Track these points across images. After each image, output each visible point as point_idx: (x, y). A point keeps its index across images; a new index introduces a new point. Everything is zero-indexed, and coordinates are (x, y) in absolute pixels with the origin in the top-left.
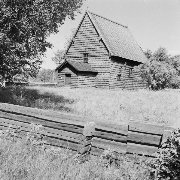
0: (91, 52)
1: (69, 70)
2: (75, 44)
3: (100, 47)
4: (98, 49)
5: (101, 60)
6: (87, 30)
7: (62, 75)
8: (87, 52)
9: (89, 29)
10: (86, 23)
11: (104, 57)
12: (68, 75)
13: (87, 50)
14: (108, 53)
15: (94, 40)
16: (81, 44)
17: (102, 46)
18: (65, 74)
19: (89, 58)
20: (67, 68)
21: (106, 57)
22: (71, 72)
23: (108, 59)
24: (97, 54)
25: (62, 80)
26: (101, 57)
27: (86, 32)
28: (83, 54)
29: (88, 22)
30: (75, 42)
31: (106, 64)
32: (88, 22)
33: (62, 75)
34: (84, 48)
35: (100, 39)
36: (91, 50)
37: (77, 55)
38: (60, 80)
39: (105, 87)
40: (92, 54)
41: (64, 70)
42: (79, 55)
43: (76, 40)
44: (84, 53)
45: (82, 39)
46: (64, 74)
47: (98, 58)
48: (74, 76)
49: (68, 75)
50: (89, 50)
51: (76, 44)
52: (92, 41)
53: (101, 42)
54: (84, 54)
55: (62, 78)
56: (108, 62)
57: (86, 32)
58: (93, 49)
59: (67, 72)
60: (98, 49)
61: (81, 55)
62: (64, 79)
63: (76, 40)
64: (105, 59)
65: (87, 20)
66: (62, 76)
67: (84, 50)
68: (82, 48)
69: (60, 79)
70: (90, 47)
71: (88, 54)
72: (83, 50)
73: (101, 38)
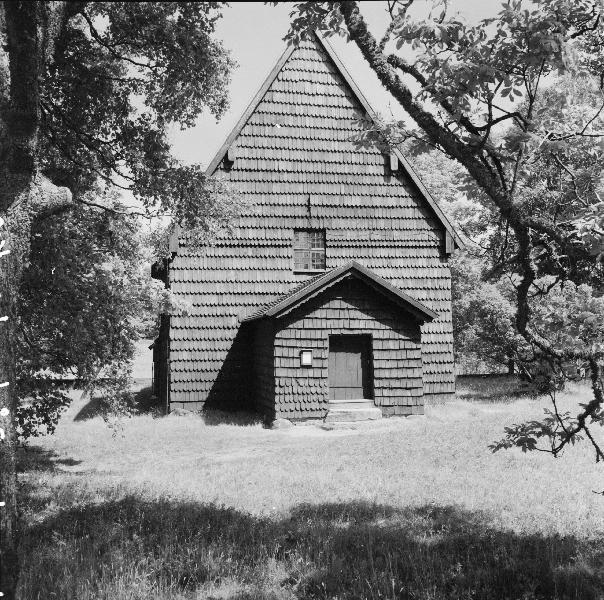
0: (342, 223)
1: (358, 314)
2: (235, 175)
3: (392, 202)
4: (379, 213)
5: (401, 262)
6: (314, 111)
7: (304, 344)
8: (315, 224)
9: (324, 112)
10: (306, 76)
11: (412, 252)
12: (340, 343)
13: (314, 212)
14: (433, 235)
15: (356, 169)
16: (275, 177)
17: (403, 202)
18: (333, 338)
19: (330, 252)
20: (336, 304)
21: (425, 252)
22: (371, 324)
23: (437, 262)
24: (377, 236)
25: (310, 373)
26: (398, 252)
27: (309, 122)
28: (292, 231)
29: (315, 77)
30: (234, 166)
31: (429, 284)
32: (315, 77)
33: (304, 344)
34: (302, 200)
35: (394, 166)
36: (343, 212)
37: (251, 234)
38: (299, 373)
39: (437, 388)
40: (350, 235)
41: (318, 313)
42: (261, 234)
43: (246, 153)
44: (300, 224)
45: (285, 154)
46: (318, 334)
47: (384, 252)
48: (391, 345)
49: (360, 345)
50: (332, 212)
51: (245, 176)
52: (346, 169)
53: (394, 181)
54: (297, 230)
55: (307, 359)
56: (436, 273)
57: (309, 122)
58: (349, 213)
59: (337, 324)
60: (379, 213)
61: (278, 234)
62: (326, 364)
63: (246, 153)
64: (421, 262)
65: (308, 65)
66: (309, 350)
67: (302, 212)
68: (288, 199)
69: (296, 363)
70: (336, 201)
71: (323, 231)
72: (288, 212)
73: (400, 162)
